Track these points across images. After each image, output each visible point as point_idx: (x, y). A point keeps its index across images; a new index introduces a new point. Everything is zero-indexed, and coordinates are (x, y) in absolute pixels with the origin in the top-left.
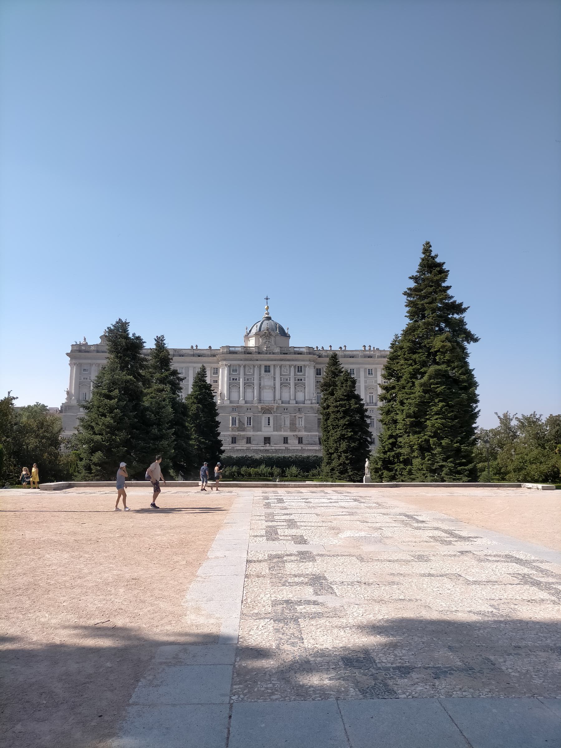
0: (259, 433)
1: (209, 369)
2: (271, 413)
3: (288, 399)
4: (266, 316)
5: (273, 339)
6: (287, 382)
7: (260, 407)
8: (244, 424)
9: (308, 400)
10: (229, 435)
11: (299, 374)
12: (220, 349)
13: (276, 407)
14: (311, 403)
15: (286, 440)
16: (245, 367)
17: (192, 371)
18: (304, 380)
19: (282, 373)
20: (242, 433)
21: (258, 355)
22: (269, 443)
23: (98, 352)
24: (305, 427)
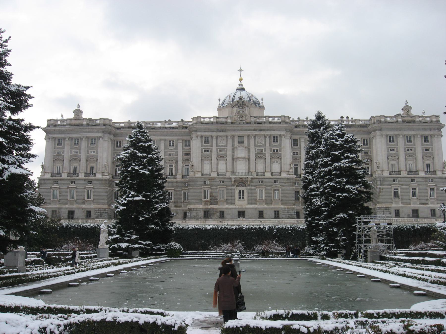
0: (232, 207)
1: (181, 141)
2: (246, 186)
3: (263, 171)
5: (247, 108)
6: (261, 152)
7: (233, 180)
8: (215, 198)
10: (202, 209)
11: (274, 144)
12: (191, 120)
13: (250, 179)
15: (261, 215)
17: (164, 144)
18: (281, 151)
19: (257, 144)
20: (214, 207)
22: (244, 217)
24: (282, 200)
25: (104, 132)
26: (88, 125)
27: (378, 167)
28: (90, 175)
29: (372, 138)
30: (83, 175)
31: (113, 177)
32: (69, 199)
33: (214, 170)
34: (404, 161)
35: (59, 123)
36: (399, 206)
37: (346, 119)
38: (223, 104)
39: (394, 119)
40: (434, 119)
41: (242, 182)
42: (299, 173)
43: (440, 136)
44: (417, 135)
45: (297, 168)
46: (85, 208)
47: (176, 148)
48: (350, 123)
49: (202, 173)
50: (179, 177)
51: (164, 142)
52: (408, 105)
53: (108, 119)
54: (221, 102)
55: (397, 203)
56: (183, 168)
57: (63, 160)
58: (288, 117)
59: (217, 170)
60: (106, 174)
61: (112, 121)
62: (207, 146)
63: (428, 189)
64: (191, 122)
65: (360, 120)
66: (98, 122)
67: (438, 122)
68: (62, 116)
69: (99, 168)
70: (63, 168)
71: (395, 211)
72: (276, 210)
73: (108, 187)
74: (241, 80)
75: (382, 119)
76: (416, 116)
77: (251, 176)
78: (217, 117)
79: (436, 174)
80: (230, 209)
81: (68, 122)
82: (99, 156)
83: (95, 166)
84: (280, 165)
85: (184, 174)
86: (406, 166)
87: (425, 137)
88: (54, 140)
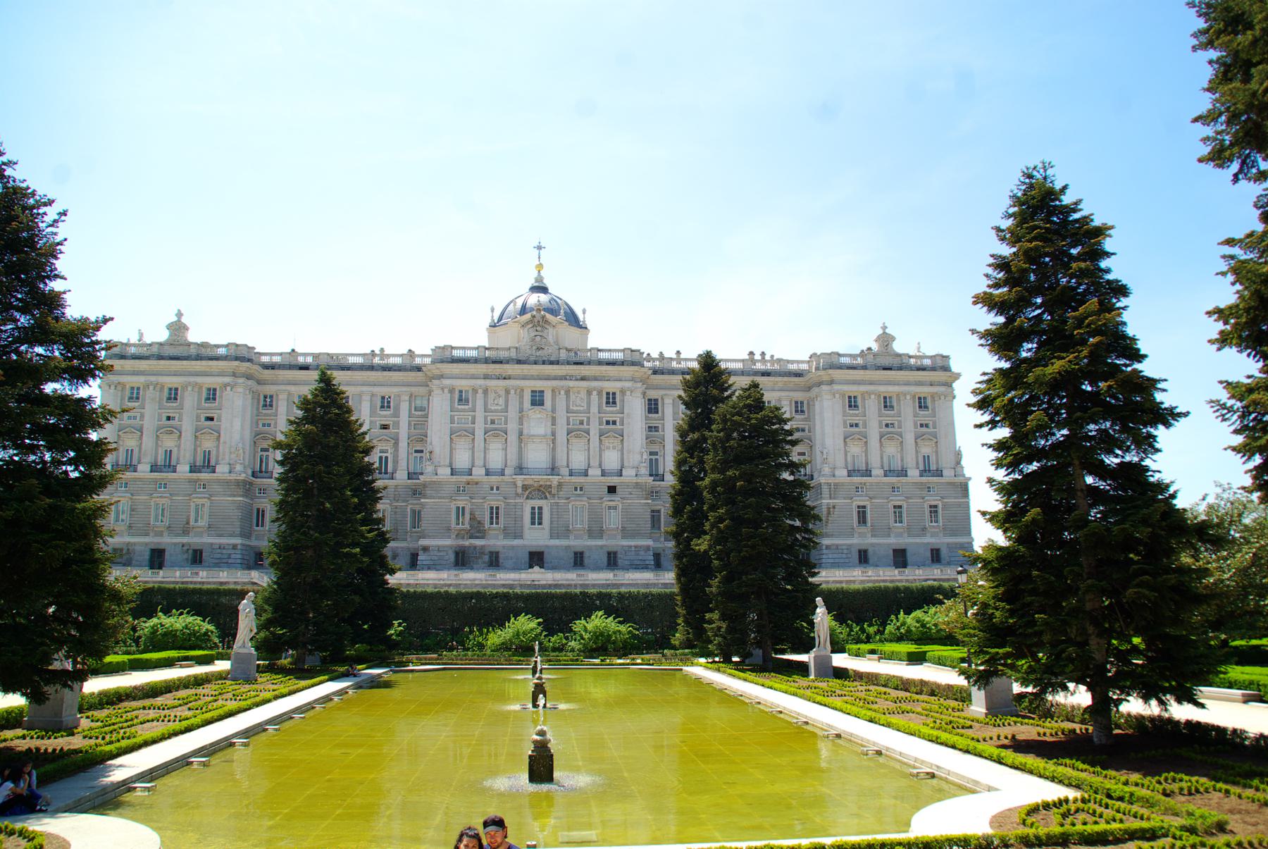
0: (516, 542)
1: (407, 398)
2: (546, 498)
3: (583, 466)
4: (537, 284)
7: (520, 484)
8: (479, 522)
9: (629, 467)
10: (450, 547)
11: (608, 409)
12: (430, 353)
13: (555, 483)
14: (636, 475)
16: (486, 392)
19: (571, 407)
21: (517, 366)
22: (542, 567)
23: (160, 358)
24: (624, 529)
25: (234, 375)
26: (199, 358)
27: (825, 461)
28: (203, 470)
29: (813, 400)
30: (188, 468)
31: (254, 474)
32: (152, 523)
33: (479, 462)
34: (878, 448)
35: (133, 350)
36: (866, 542)
37: (759, 358)
38: (500, 318)
39: (860, 361)
40: (939, 363)
41: (539, 490)
42: (661, 472)
43: (951, 398)
44: (905, 395)
45: (657, 460)
46: (189, 544)
47: (396, 415)
48: (769, 366)
49: (452, 469)
50: (401, 475)
51: (369, 398)
52: (887, 331)
53: (246, 345)
54: (496, 315)
55: (862, 535)
56: (410, 456)
57: (142, 435)
58: (639, 351)
59: (485, 463)
60: (239, 468)
61: (256, 351)
62: (464, 410)
63: (925, 506)
64: (429, 356)
65: (788, 362)
66: (222, 351)
67: (946, 369)
68: (141, 335)
69: (224, 455)
70: (140, 452)
71: (860, 551)
72: (610, 550)
73: (243, 496)
74: (540, 267)
75: (835, 359)
76: (904, 354)
77: (557, 477)
78: (486, 349)
79: (942, 476)
80: (513, 547)
81: (155, 350)
82: (223, 427)
83: (215, 449)
84: (619, 453)
85: (411, 470)
86: (882, 458)
87: (920, 398)
88: (119, 388)
